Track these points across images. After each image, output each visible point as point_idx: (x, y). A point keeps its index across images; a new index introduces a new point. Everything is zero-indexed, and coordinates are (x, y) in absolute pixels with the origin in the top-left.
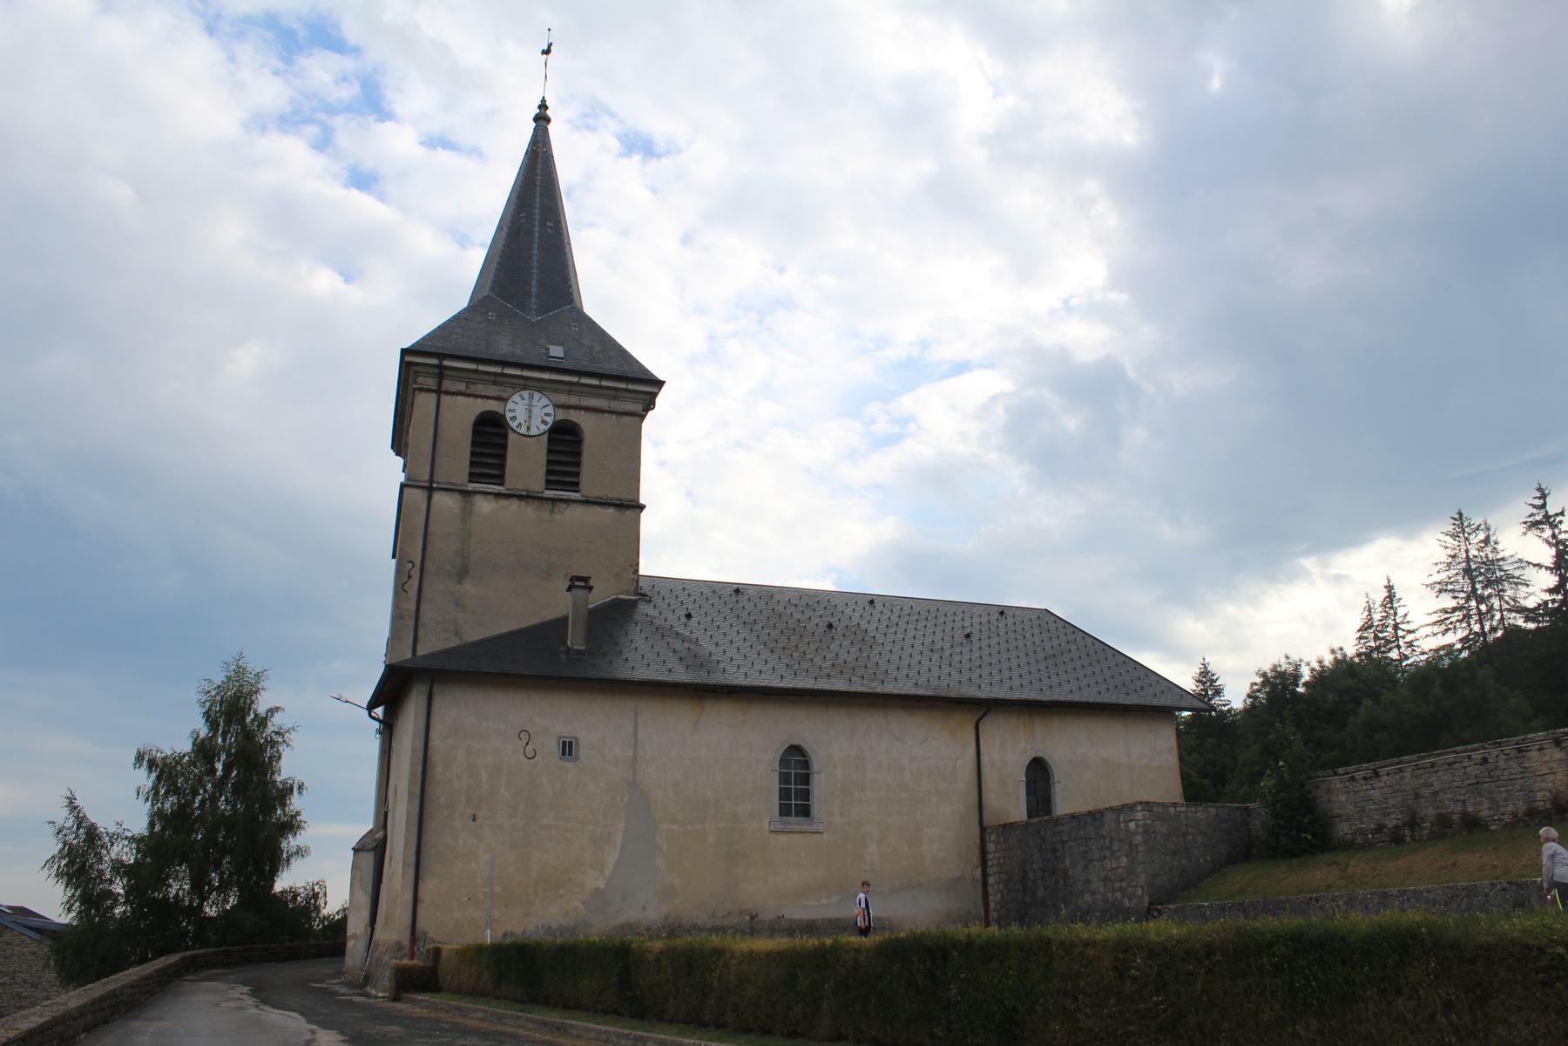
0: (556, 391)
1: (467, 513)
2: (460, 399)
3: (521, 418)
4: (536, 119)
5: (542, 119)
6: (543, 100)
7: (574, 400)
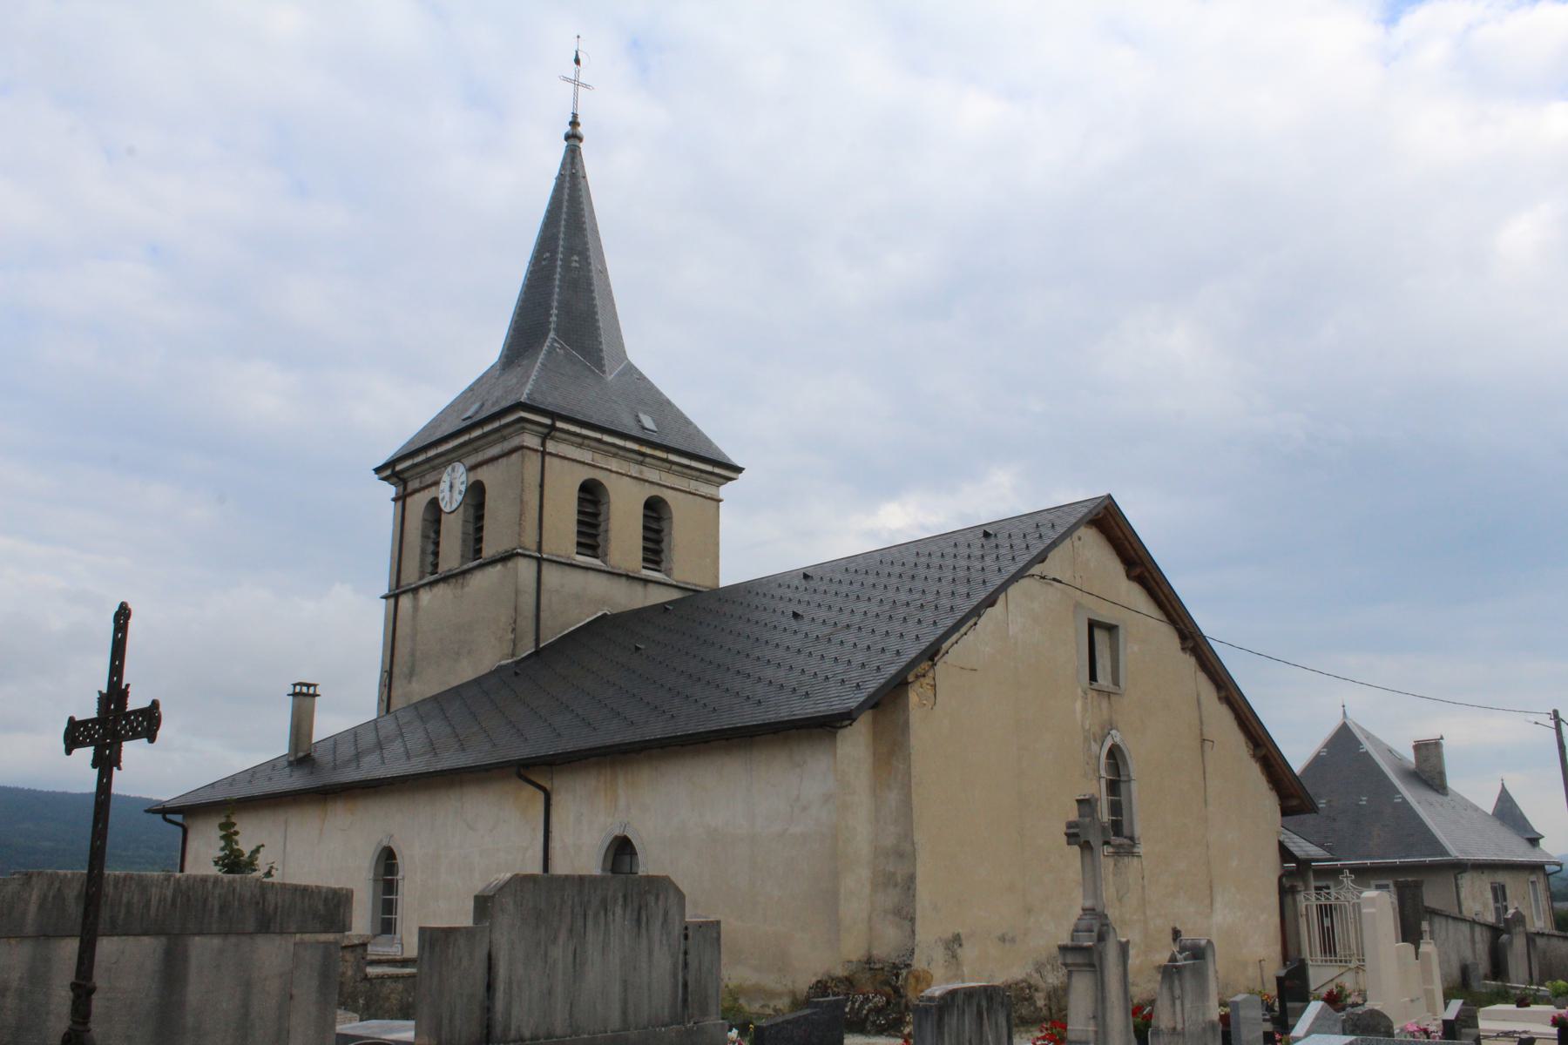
0: (469, 454)
1: (416, 608)
2: (417, 496)
3: (447, 494)
4: (568, 137)
5: (573, 138)
6: (575, 116)
7: (480, 457)
